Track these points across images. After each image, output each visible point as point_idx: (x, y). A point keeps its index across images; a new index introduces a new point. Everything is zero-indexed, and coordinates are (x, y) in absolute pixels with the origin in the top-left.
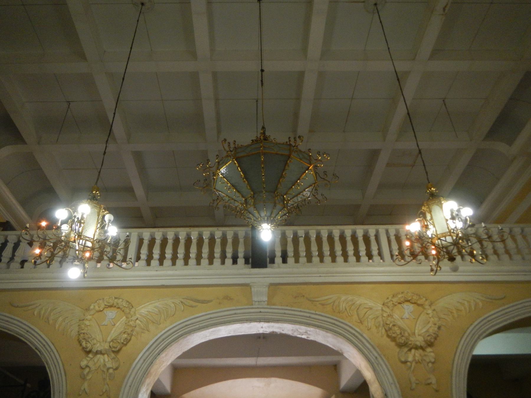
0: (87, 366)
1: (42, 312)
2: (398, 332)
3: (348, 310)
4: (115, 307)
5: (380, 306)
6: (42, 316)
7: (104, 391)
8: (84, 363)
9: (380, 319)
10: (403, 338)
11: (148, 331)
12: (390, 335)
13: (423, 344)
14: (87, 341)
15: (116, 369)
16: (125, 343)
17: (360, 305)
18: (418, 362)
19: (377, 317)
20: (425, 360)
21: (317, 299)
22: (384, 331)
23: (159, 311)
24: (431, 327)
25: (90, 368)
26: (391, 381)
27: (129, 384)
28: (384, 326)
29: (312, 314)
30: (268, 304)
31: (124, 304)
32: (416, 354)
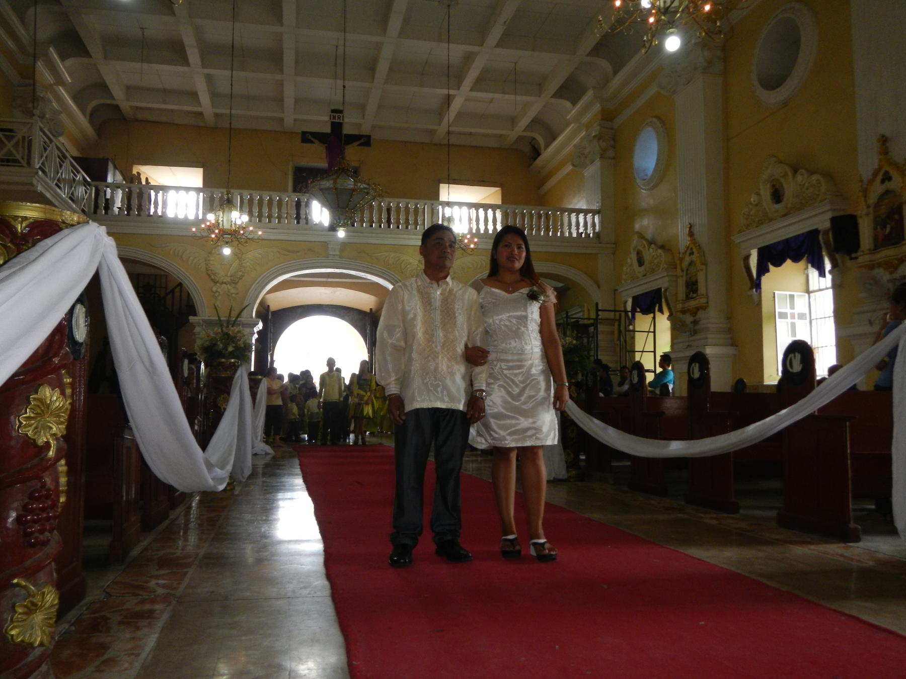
0: (217, 291)
8: (214, 289)
9: (415, 271)
15: (237, 294)
25: (219, 293)
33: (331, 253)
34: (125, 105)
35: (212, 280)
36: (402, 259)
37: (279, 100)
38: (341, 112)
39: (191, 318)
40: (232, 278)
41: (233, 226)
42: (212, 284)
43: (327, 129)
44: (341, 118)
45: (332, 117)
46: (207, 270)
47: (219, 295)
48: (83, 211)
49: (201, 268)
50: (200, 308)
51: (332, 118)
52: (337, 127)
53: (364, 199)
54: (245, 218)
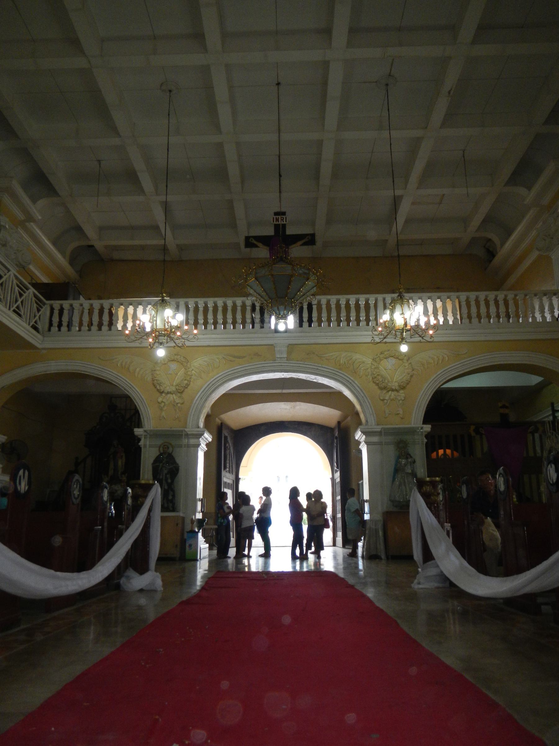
0: (162, 402)
1: (124, 364)
2: (381, 380)
3: (346, 363)
4: (176, 361)
5: (369, 361)
6: (124, 367)
7: (176, 417)
8: (160, 400)
9: (369, 370)
10: (383, 384)
11: (202, 378)
12: (375, 381)
13: (397, 388)
14: (160, 385)
15: (182, 404)
16: (186, 386)
17: (356, 360)
18: (392, 400)
19: (367, 369)
20: (397, 399)
21: (324, 356)
22: (371, 378)
23: (208, 364)
24: (405, 376)
25: (164, 403)
26: (371, 413)
27: (192, 414)
28: (371, 375)
29: (320, 367)
30: (287, 360)
31: (182, 359)
32: (392, 395)
33: (278, 356)
34: (99, 245)
35: (158, 390)
36: (354, 358)
37: (233, 225)
38: (284, 214)
39: (138, 431)
40: (177, 387)
41: (166, 325)
42: (158, 394)
43: (270, 231)
44: (284, 220)
45: (275, 219)
46: (153, 381)
47: (164, 406)
48: (35, 328)
49: (147, 378)
50: (146, 419)
51: (275, 221)
52: (280, 229)
53: (305, 286)
54: (181, 317)
